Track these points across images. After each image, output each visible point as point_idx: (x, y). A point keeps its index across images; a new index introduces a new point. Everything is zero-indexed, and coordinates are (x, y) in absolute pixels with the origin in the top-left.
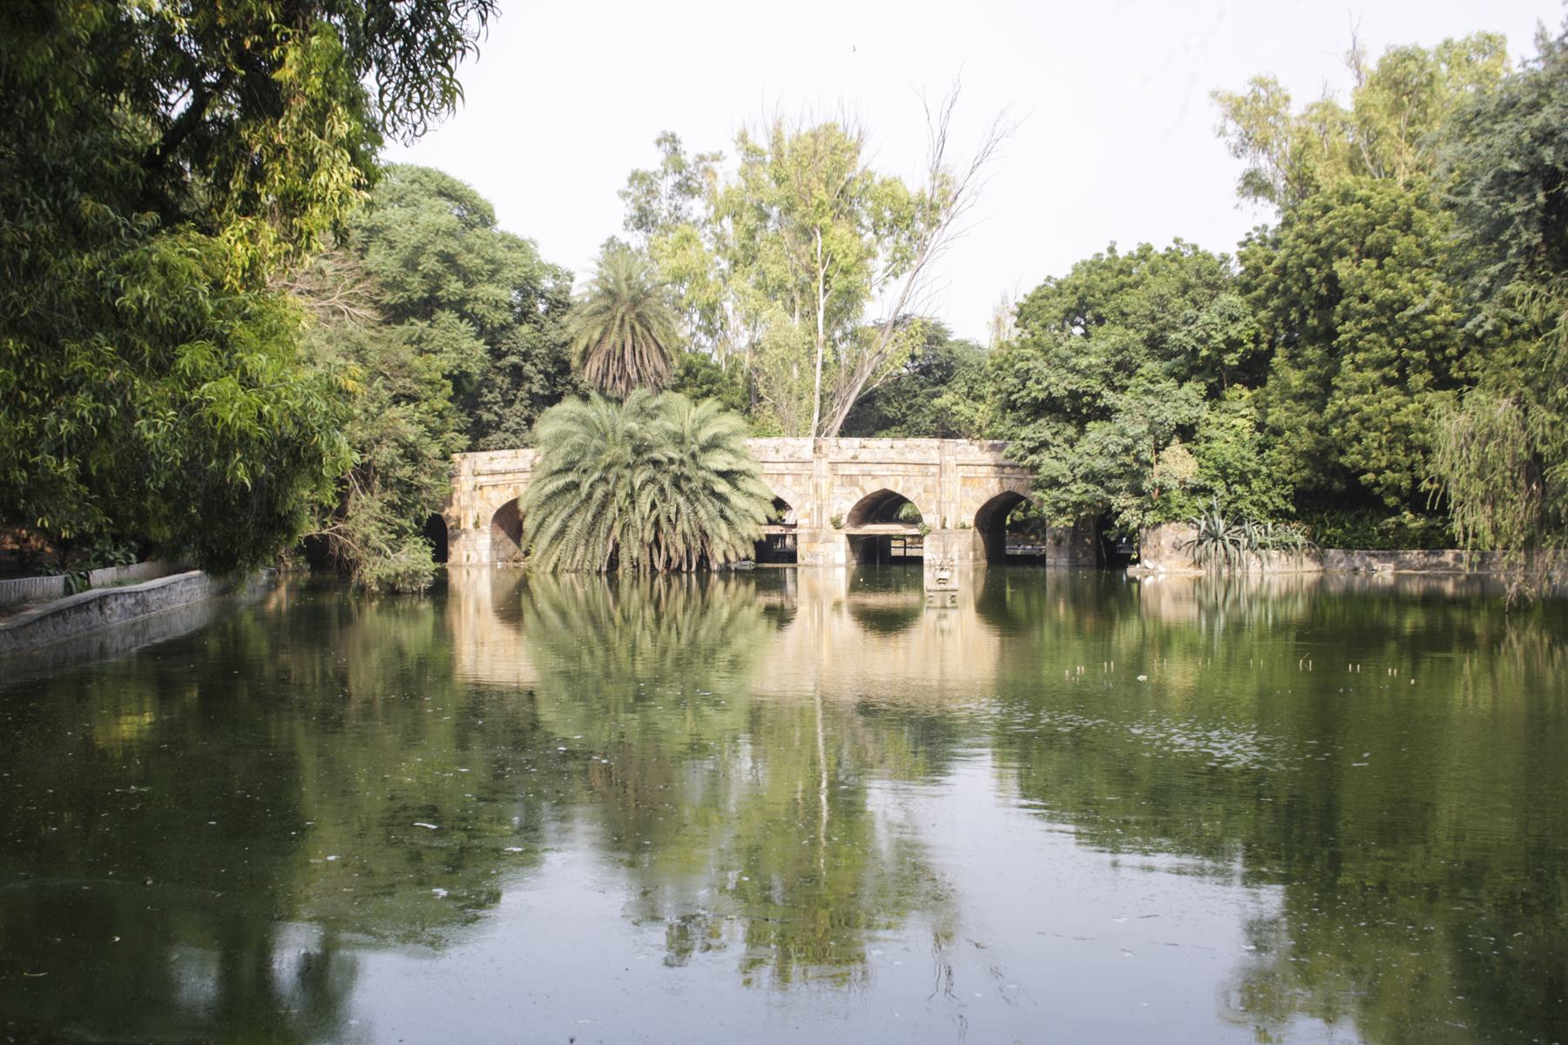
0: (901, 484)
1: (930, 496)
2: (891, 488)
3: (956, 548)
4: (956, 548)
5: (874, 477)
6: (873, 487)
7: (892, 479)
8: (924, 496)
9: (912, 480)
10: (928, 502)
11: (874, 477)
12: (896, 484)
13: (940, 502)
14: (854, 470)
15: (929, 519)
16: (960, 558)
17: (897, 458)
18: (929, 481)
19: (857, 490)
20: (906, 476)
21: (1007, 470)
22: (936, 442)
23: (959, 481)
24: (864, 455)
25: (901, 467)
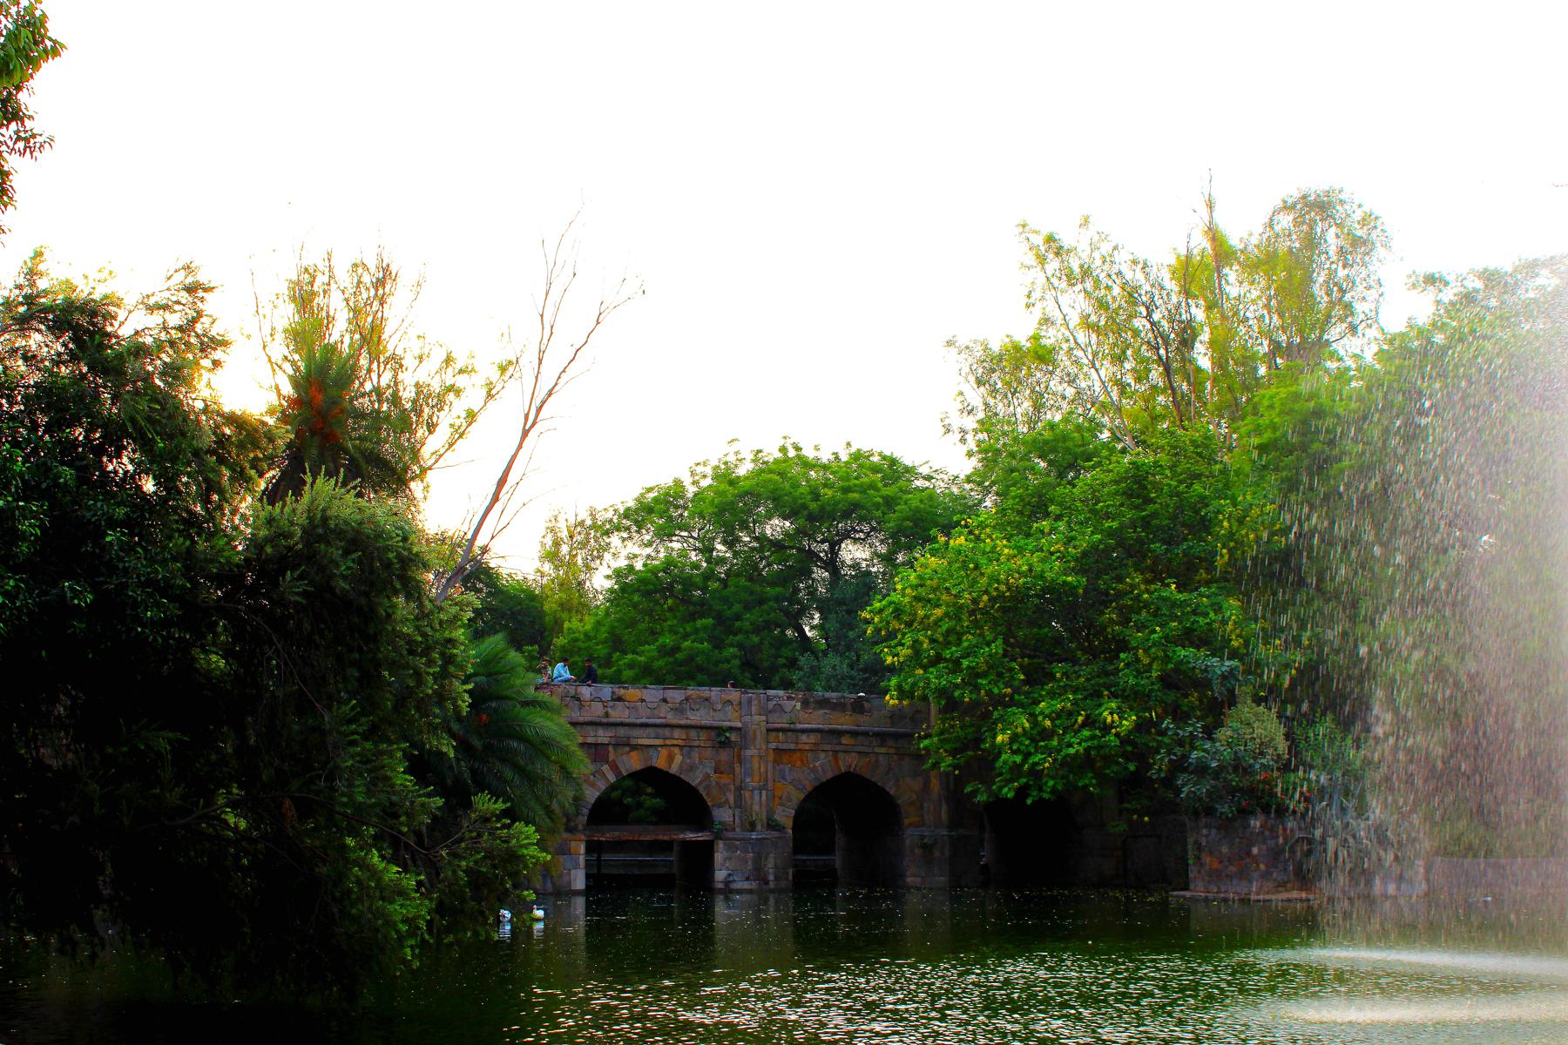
0: (678, 758)
1: (725, 779)
2: (660, 762)
3: (771, 863)
4: (771, 863)
5: (634, 747)
6: (632, 762)
7: (664, 752)
8: (714, 777)
9: (695, 754)
10: (722, 788)
11: (634, 747)
12: (671, 758)
13: (739, 789)
14: (603, 736)
15: (723, 815)
16: (777, 878)
17: (672, 718)
18: (724, 755)
19: (605, 768)
20: (687, 748)
21: (845, 740)
22: (734, 694)
23: (771, 757)
24: (619, 713)
25: (677, 733)
